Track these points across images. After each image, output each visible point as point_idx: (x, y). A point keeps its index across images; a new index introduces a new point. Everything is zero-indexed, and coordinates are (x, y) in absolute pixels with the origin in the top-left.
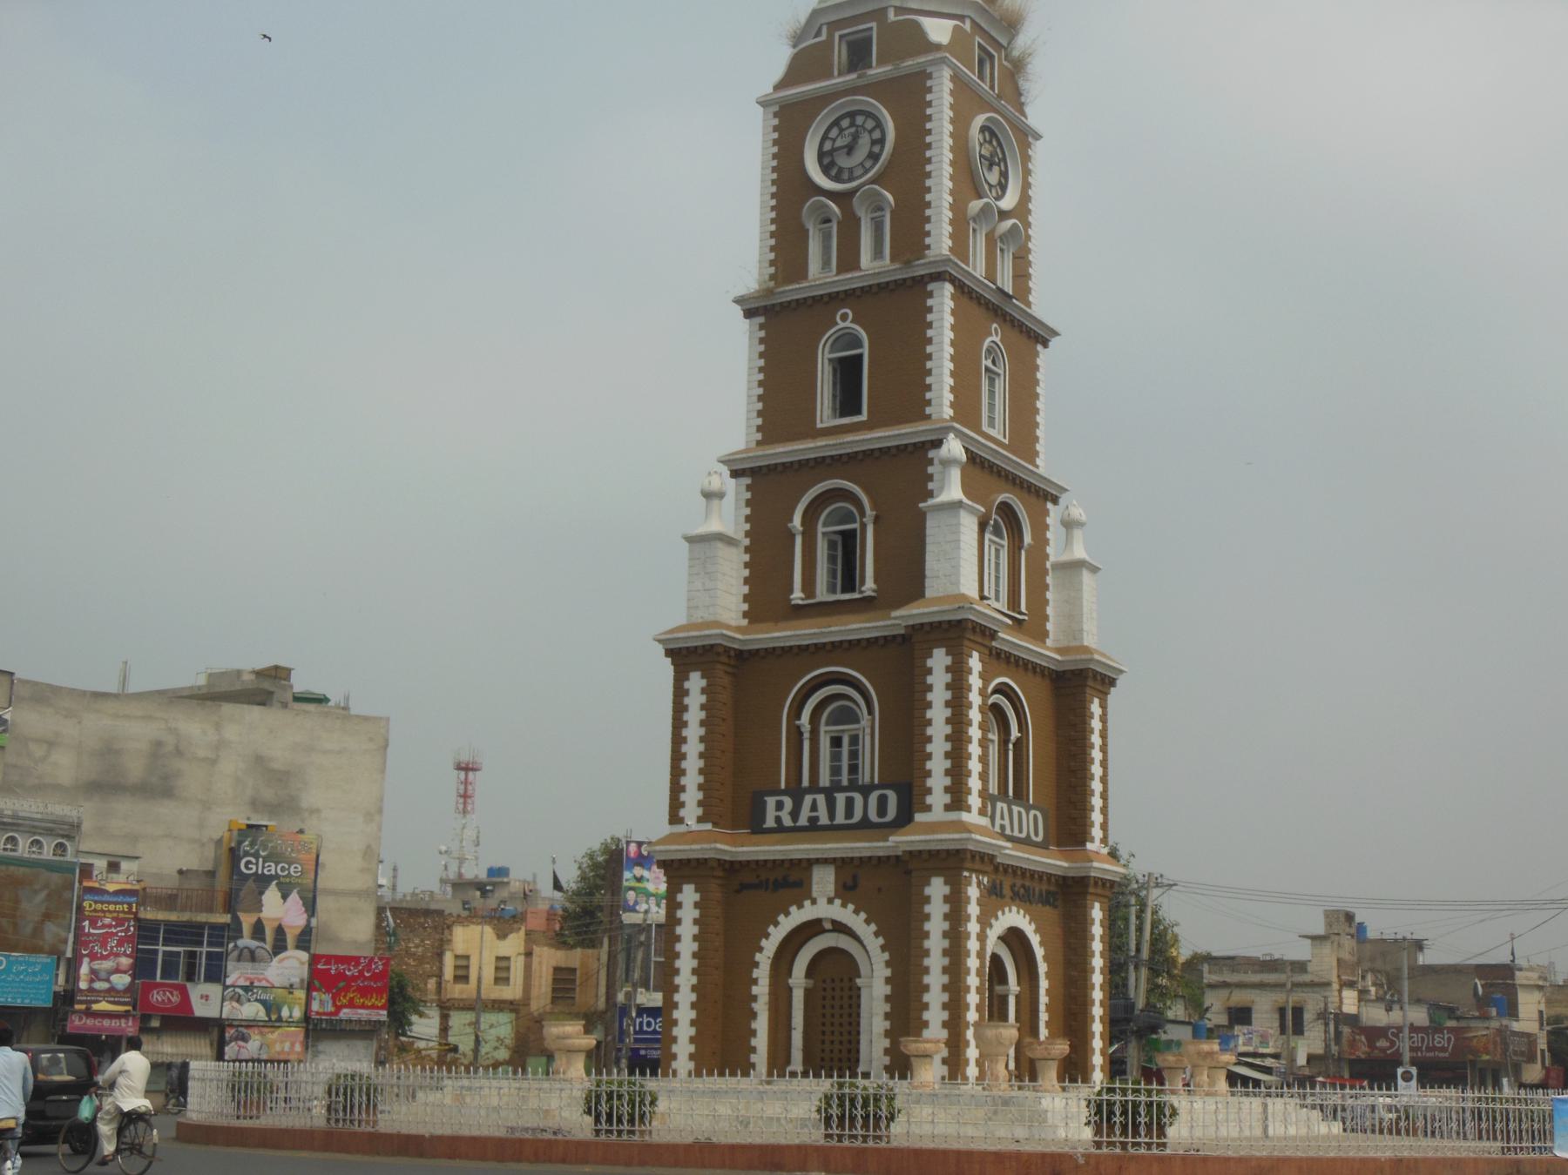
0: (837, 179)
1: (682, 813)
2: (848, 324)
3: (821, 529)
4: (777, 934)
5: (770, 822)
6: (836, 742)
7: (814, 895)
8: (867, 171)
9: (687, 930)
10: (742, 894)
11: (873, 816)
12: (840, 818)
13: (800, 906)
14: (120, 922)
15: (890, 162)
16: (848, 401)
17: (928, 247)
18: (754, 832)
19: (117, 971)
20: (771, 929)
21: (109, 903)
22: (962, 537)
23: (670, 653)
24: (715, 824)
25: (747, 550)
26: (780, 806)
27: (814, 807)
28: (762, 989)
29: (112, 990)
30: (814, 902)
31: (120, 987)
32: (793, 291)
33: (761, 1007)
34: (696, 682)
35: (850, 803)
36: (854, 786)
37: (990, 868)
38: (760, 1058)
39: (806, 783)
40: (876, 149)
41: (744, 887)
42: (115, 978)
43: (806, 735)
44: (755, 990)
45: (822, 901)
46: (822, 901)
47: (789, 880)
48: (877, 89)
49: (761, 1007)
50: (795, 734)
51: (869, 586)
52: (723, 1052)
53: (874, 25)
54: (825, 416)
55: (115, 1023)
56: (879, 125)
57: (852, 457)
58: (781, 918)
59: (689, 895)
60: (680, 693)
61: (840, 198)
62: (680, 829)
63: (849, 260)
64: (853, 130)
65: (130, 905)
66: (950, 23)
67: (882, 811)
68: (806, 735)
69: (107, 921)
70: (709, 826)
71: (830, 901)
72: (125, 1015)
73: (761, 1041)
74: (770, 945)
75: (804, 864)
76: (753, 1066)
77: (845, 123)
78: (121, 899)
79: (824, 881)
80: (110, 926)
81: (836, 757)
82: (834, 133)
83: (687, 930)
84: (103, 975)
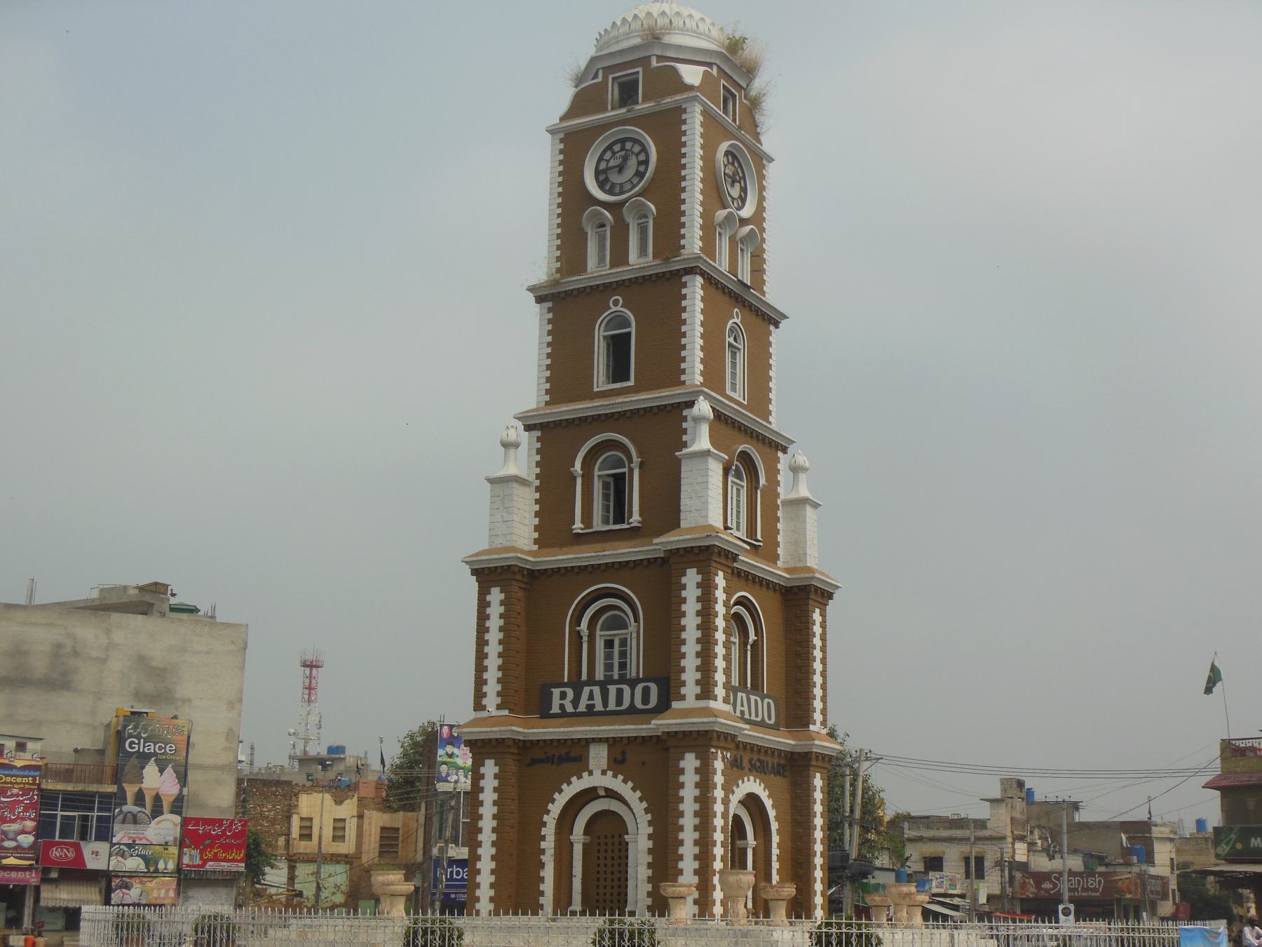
0: (610, 192)
1: (484, 701)
2: (618, 308)
3: (597, 473)
4: (561, 800)
5: (555, 709)
6: (609, 644)
7: (591, 767)
8: (634, 186)
9: (488, 796)
10: (533, 767)
11: (638, 704)
12: (612, 706)
13: (580, 777)
14: (26, 792)
15: (653, 179)
16: (619, 370)
17: (683, 247)
18: (542, 717)
19: (23, 832)
20: (556, 796)
21: (17, 776)
22: (710, 480)
23: (475, 572)
24: (511, 711)
25: (538, 489)
26: (563, 696)
27: (591, 697)
28: (548, 844)
29: (18, 848)
30: (591, 773)
31: (25, 845)
32: (575, 282)
33: (548, 859)
34: (496, 596)
35: (620, 693)
36: (623, 680)
37: (732, 746)
38: (547, 900)
39: (584, 677)
40: (642, 169)
41: (534, 761)
42: (21, 838)
43: (585, 639)
44: (543, 845)
45: (597, 773)
46: (597, 773)
47: (571, 756)
48: (639, 121)
49: (548, 859)
50: (577, 637)
51: (636, 518)
52: (517, 896)
53: (640, 69)
54: (600, 381)
55: (20, 875)
56: (644, 149)
57: (622, 414)
58: (564, 786)
59: (490, 768)
60: (483, 605)
61: (614, 207)
62: (484, 714)
63: (620, 257)
64: (623, 153)
65: (34, 778)
66: (702, 69)
67: (646, 700)
68: (585, 639)
69: (15, 791)
70: (506, 712)
71: (604, 773)
72: (30, 868)
73: (548, 887)
74: (555, 809)
75: (583, 743)
76: (542, 907)
77: (617, 148)
78: (26, 773)
79: (598, 756)
80: (18, 795)
81: (609, 656)
82: (608, 155)
83: (488, 796)
84: (11, 835)
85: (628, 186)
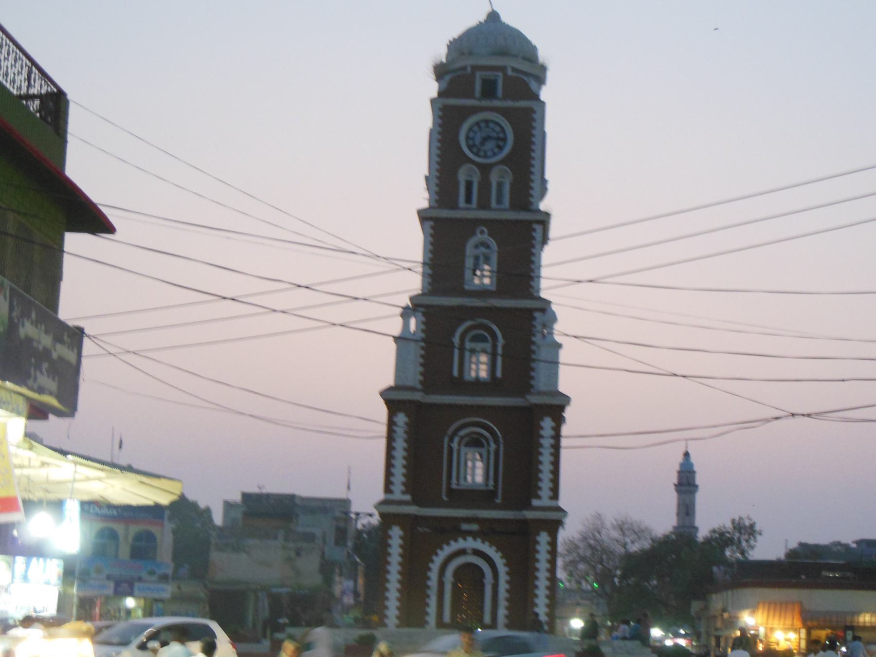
1: (392, 488)
8: (495, 154)
28: (433, 583)
40: (501, 143)
51: (499, 374)
59: (396, 532)
60: (391, 424)
76: (427, 623)
85: (490, 153)
